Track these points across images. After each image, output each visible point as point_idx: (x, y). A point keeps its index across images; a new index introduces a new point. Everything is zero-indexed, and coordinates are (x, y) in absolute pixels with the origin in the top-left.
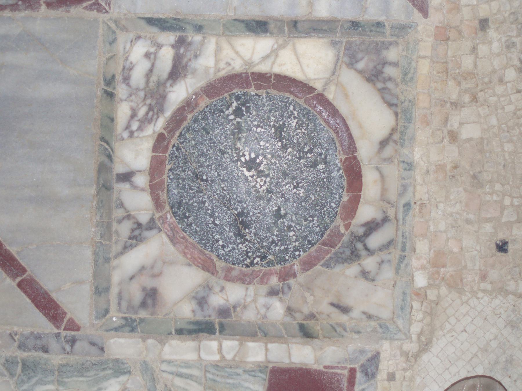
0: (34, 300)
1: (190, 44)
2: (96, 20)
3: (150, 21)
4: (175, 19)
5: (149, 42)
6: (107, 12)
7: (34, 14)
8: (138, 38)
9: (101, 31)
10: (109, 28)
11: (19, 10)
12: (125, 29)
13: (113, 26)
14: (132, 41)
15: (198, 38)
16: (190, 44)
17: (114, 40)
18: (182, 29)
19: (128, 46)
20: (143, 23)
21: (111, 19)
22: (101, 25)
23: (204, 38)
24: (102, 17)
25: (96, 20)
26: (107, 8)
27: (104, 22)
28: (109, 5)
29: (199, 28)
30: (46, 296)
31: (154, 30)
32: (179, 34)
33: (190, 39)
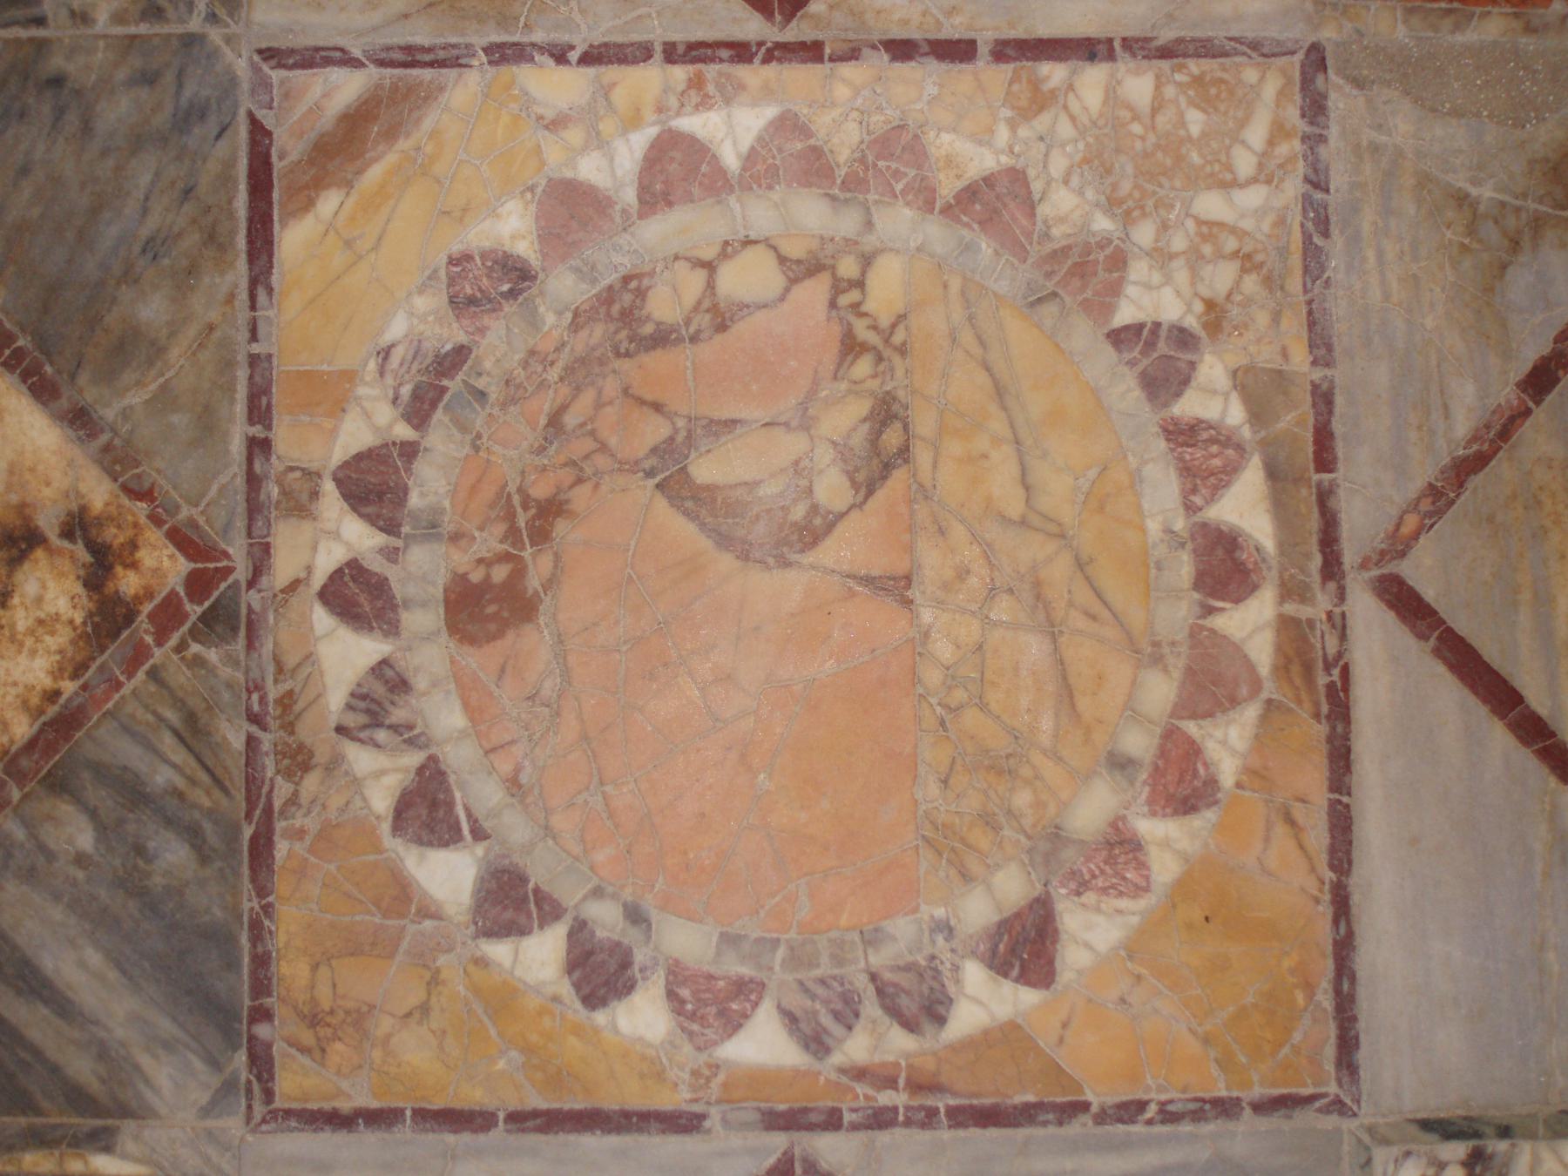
0: (544, 1129)
1: (1491, 1157)
2: (1338, 1131)
3: (1427, 1125)
4: (1465, 1118)
5: (1424, 1160)
6: (1355, 1115)
7: (1231, 1125)
8: (1408, 1154)
9: (1346, 1148)
10: (1359, 1141)
11: (1206, 1120)
12: (1386, 1142)
13: (1366, 1139)
14: (1396, 1161)
15: (1502, 1146)
16: (1491, 1157)
17: (1369, 1161)
18: (1476, 1135)
19: (1391, 1168)
20: (1414, 1130)
21: (1362, 1126)
22: (1346, 1137)
23: (1513, 1145)
24: (1348, 1124)
25: (1338, 1131)
26: (1355, 1108)
27: (1350, 1131)
28: (1358, 1102)
29: (1505, 1132)
30: (689, 504)
31: (1434, 1137)
32: (1472, 1143)
33: (1490, 1150)
